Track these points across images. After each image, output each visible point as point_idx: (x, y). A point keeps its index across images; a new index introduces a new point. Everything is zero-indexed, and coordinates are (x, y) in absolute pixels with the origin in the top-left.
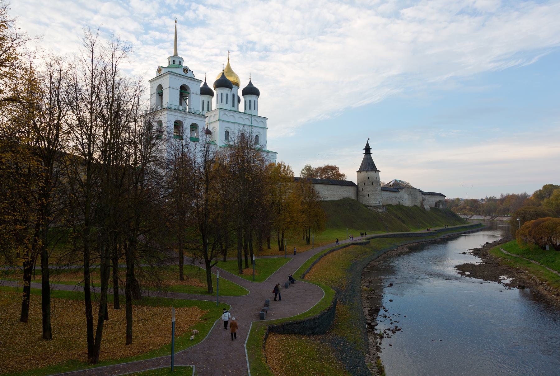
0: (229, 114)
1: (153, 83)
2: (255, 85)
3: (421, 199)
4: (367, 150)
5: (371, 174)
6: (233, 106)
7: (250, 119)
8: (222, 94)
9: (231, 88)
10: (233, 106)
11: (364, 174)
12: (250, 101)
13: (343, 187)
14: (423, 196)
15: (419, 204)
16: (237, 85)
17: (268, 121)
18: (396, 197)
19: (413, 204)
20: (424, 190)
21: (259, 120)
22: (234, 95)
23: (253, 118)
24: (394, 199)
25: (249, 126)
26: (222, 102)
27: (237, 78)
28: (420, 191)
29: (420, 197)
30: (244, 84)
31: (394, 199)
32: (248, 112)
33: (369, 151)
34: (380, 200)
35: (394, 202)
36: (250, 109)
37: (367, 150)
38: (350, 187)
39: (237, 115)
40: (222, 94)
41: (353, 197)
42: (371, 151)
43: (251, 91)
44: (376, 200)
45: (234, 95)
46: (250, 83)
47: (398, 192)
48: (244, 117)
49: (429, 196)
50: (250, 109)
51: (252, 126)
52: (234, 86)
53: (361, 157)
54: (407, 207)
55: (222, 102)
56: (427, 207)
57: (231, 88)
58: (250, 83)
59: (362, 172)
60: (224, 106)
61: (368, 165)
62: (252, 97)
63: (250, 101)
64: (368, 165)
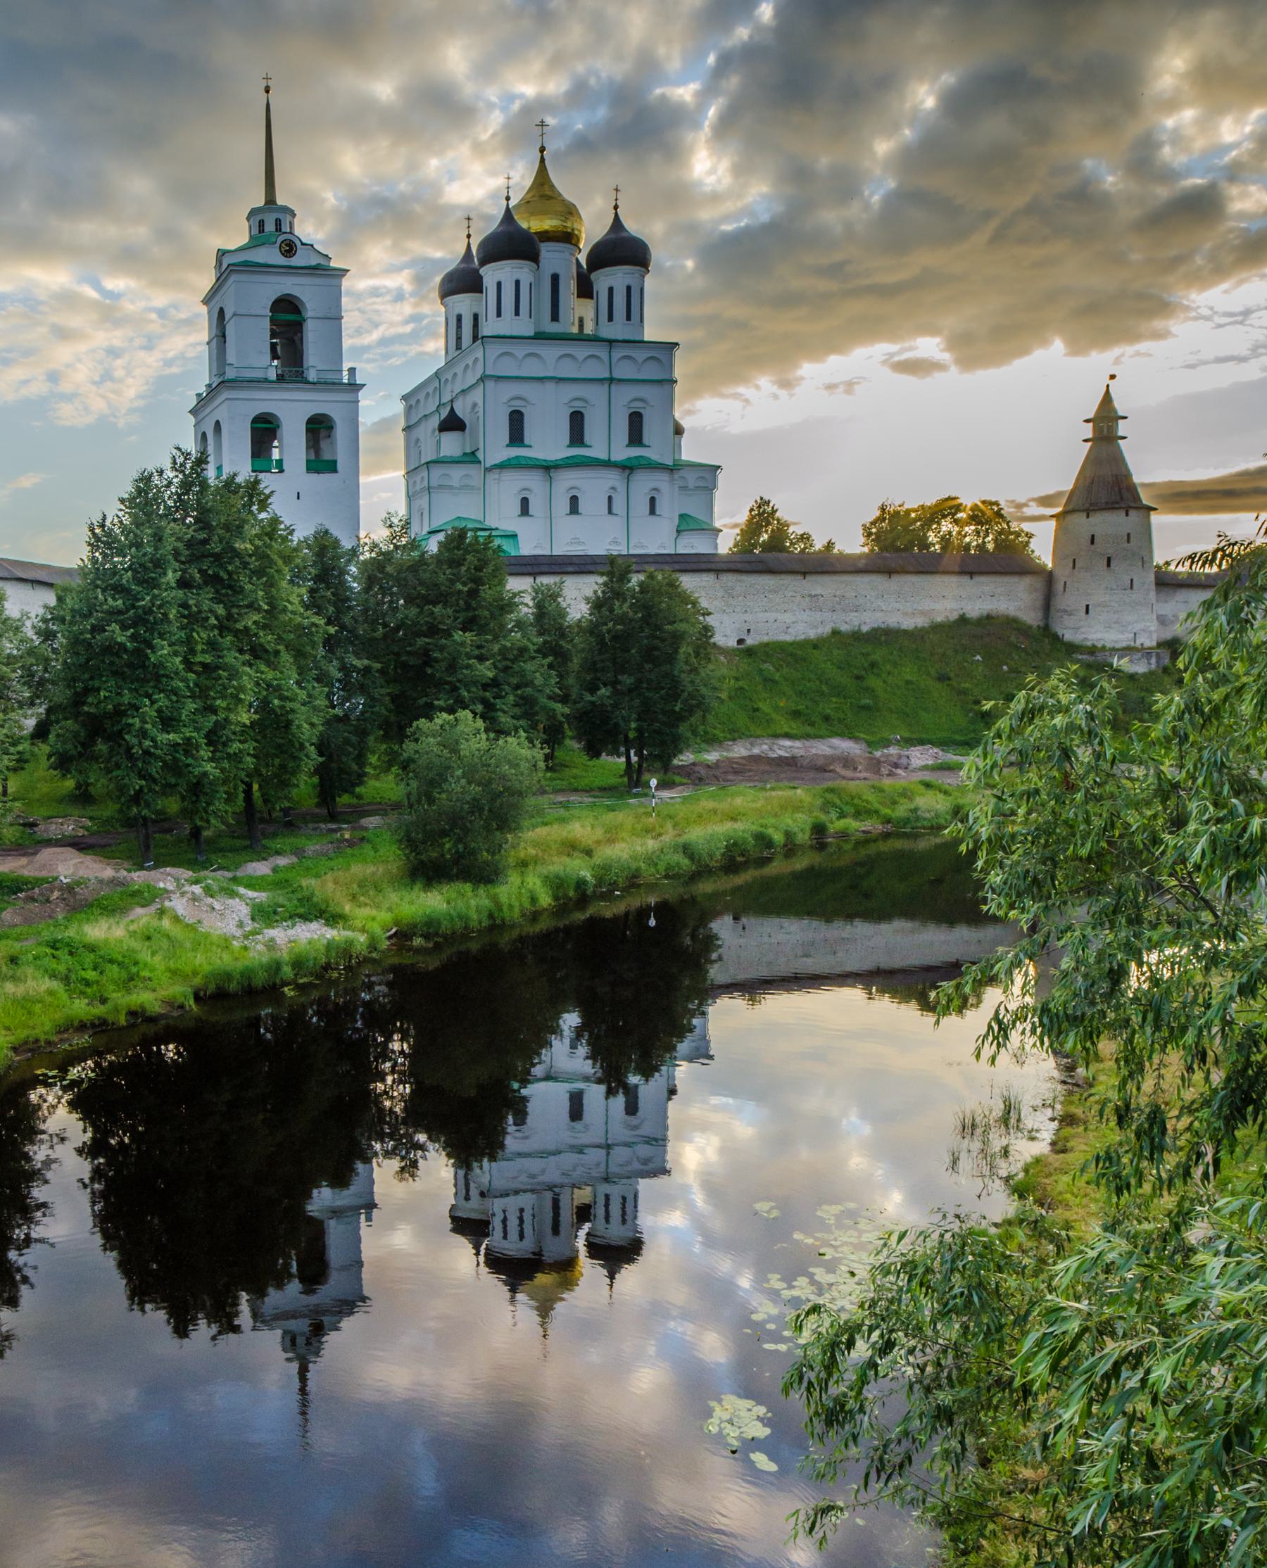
0: (520, 350)
1: (212, 304)
8: (499, 284)
11: (1082, 524)
13: (978, 579)
17: (678, 354)
21: (640, 355)
23: (618, 353)
26: (499, 315)
27: (570, 211)
32: (608, 331)
36: (610, 319)
40: (499, 284)
41: (1031, 618)
48: (581, 352)
50: (610, 319)
51: (611, 380)
55: (499, 315)
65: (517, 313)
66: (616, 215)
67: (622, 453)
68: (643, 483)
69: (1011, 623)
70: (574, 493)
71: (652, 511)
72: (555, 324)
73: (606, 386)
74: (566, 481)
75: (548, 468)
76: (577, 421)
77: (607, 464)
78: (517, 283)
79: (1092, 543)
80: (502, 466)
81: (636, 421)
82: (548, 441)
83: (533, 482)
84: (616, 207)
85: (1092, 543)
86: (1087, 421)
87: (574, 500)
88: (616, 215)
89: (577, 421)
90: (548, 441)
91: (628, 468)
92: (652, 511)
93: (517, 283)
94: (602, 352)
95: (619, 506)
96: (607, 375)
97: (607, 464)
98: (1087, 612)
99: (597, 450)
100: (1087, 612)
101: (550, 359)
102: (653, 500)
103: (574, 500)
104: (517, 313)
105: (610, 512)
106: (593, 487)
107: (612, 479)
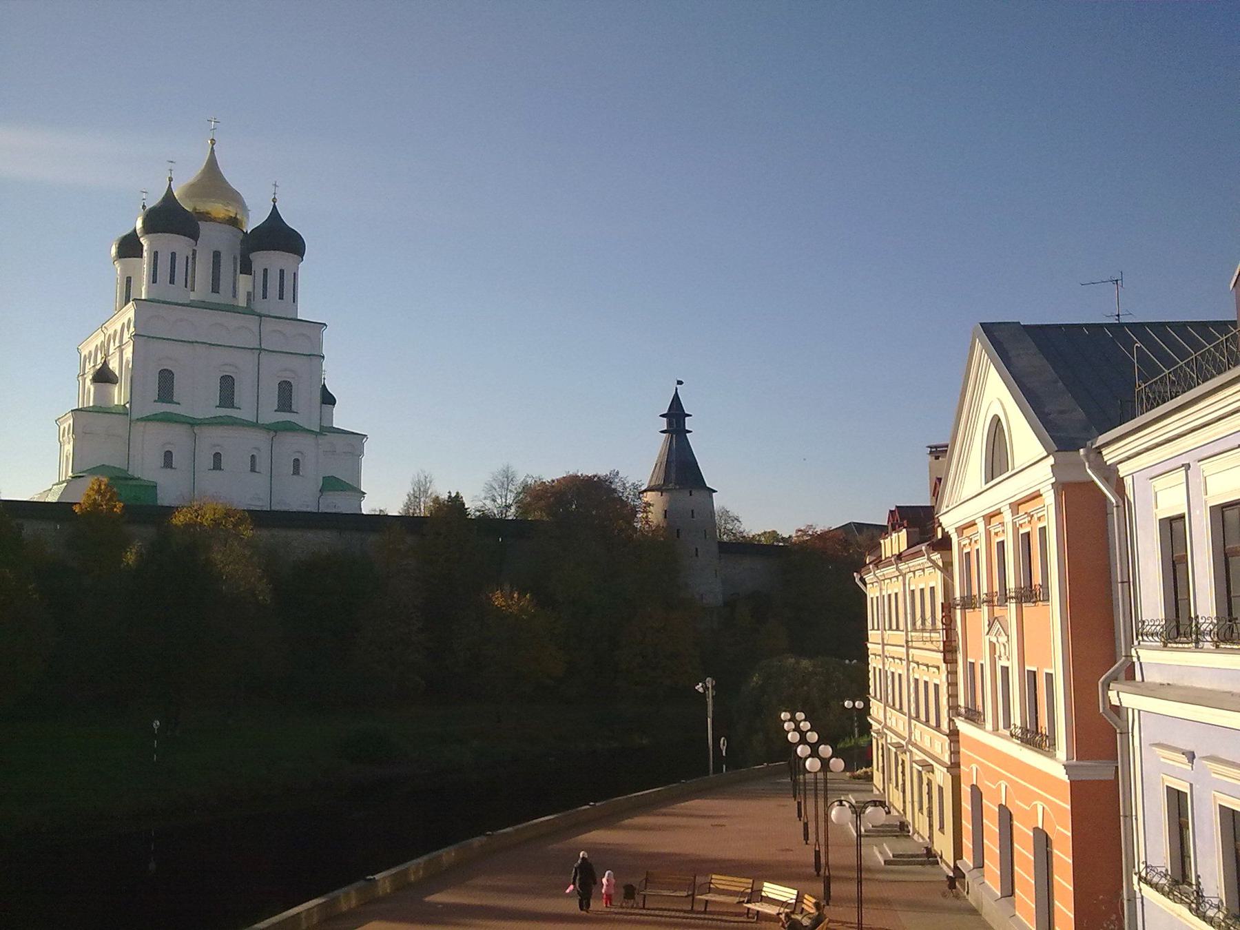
4: (676, 416)
9: (194, 235)
23: (269, 325)
32: (260, 306)
36: (265, 297)
37: (676, 416)
42: (689, 424)
51: (261, 350)
57: (194, 235)
60: (177, 293)
64: (681, 469)
65: (172, 281)
66: (274, 206)
67: (270, 415)
68: (290, 445)
70: (218, 450)
71: (296, 471)
74: (211, 438)
75: (193, 423)
76: (227, 384)
77: (255, 425)
78: (173, 254)
80: (147, 419)
81: (285, 390)
82: (196, 397)
83: (176, 436)
84: (274, 200)
87: (217, 457)
88: (274, 206)
89: (227, 384)
90: (196, 397)
91: (276, 429)
92: (296, 471)
93: (173, 254)
94: (252, 322)
95: (263, 464)
97: (255, 425)
99: (246, 414)
101: (204, 324)
102: (296, 461)
103: (217, 457)
104: (172, 281)
105: (253, 470)
106: (237, 445)
107: (259, 439)
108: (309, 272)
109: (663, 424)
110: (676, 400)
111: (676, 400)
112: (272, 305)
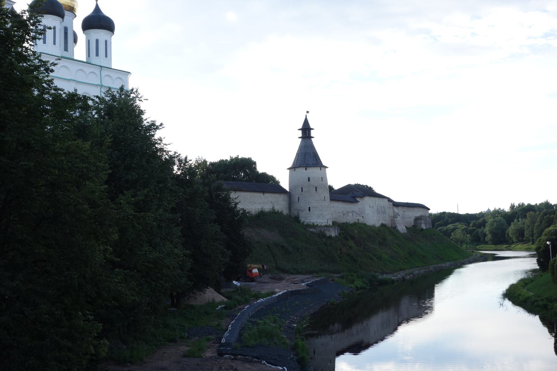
2: (106, 11)
3: (392, 214)
4: (306, 130)
5: (313, 172)
6: (66, 49)
7: (98, 72)
9: (62, 16)
10: (66, 49)
12: (97, 41)
13: (267, 195)
14: (396, 209)
15: (387, 222)
16: (72, 9)
18: (353, 212)
19: (380, 222)
20: (396, 199)
21: (114, 75)
22: (66, 29)
23: (105, 72)
24: (350, 214)
25: (97, 85)
28: (389, 200)
29: (390, 211)
30: (84, 10)
31: (350, 214)
32: (95, 60)
33: (309, 133)
34: (328, 217)
35: (350, 219)
36: (97, 55)
37: (306, 130)
38: (277, 196)
39: (74, 67)
42: (313, 133)
43: (98, 22)
44: (322, 215)
45: (66, 29)
46: (97, 9)
47: (357, 202)
48: (88, 69)
49: (404, 208)
50: (97, 55)
52: (67, 13)
53: (295, 143)
54: (372, 228)
56: (402, 228)
57: (62, 16)
58: (97, 9)
59: (297, 170)
61: (308, 157)
62: (100, 34)
63: (97, 41)
64: (308, 157)
65: (54, 44)
69: (274, 213)
72: (66, 52)
73: (99, 88)
79: (309, 181)
85: (309, 181)
86: (299, 130)
94: (97, 70)
96: (99, 83)
98: (309, 210)
100: (309, 210)
104: (54, 44)
108: (117, 41)
109: (300, 134)
110: (306, 122)
111: (306, 122)
112: (100, 60)
